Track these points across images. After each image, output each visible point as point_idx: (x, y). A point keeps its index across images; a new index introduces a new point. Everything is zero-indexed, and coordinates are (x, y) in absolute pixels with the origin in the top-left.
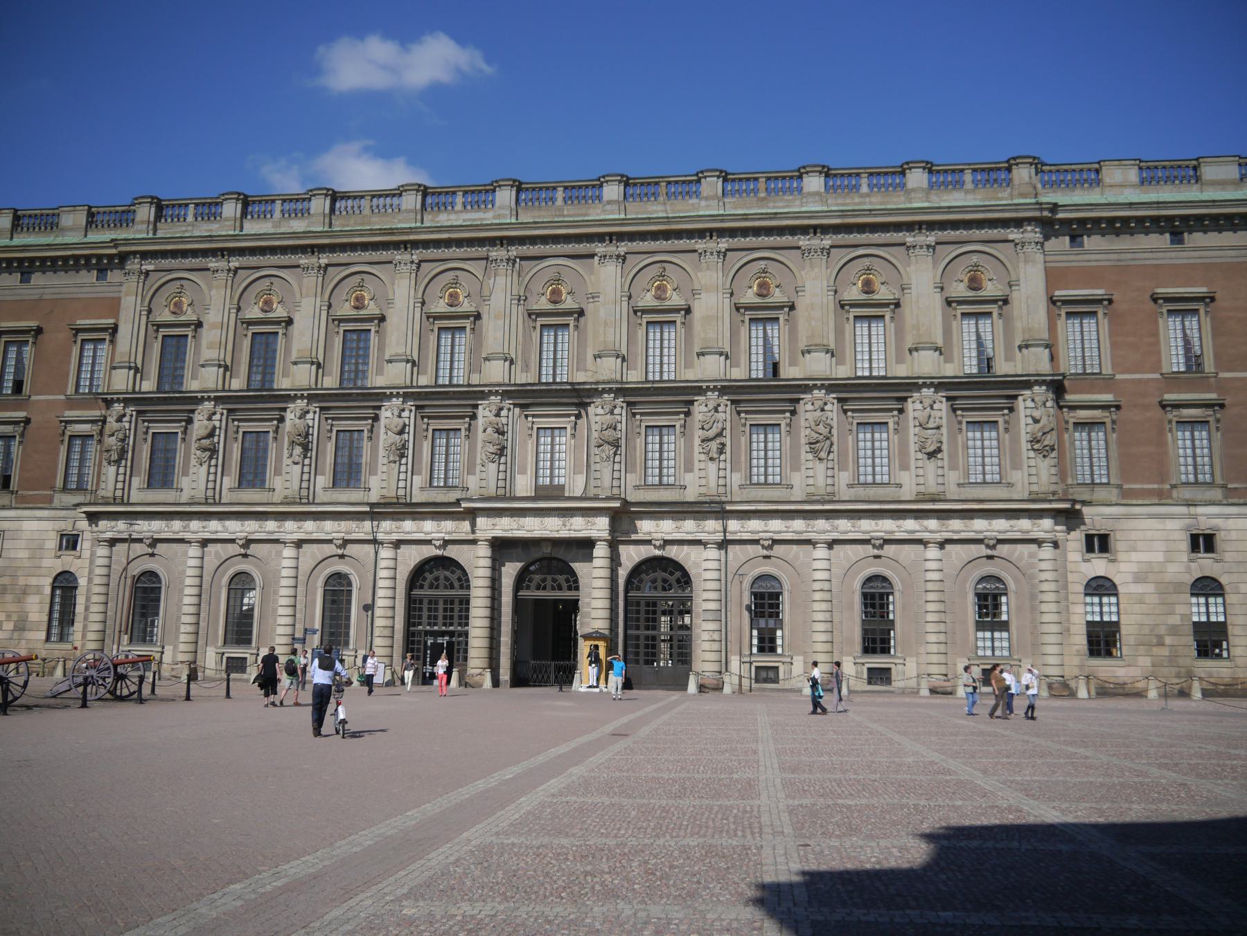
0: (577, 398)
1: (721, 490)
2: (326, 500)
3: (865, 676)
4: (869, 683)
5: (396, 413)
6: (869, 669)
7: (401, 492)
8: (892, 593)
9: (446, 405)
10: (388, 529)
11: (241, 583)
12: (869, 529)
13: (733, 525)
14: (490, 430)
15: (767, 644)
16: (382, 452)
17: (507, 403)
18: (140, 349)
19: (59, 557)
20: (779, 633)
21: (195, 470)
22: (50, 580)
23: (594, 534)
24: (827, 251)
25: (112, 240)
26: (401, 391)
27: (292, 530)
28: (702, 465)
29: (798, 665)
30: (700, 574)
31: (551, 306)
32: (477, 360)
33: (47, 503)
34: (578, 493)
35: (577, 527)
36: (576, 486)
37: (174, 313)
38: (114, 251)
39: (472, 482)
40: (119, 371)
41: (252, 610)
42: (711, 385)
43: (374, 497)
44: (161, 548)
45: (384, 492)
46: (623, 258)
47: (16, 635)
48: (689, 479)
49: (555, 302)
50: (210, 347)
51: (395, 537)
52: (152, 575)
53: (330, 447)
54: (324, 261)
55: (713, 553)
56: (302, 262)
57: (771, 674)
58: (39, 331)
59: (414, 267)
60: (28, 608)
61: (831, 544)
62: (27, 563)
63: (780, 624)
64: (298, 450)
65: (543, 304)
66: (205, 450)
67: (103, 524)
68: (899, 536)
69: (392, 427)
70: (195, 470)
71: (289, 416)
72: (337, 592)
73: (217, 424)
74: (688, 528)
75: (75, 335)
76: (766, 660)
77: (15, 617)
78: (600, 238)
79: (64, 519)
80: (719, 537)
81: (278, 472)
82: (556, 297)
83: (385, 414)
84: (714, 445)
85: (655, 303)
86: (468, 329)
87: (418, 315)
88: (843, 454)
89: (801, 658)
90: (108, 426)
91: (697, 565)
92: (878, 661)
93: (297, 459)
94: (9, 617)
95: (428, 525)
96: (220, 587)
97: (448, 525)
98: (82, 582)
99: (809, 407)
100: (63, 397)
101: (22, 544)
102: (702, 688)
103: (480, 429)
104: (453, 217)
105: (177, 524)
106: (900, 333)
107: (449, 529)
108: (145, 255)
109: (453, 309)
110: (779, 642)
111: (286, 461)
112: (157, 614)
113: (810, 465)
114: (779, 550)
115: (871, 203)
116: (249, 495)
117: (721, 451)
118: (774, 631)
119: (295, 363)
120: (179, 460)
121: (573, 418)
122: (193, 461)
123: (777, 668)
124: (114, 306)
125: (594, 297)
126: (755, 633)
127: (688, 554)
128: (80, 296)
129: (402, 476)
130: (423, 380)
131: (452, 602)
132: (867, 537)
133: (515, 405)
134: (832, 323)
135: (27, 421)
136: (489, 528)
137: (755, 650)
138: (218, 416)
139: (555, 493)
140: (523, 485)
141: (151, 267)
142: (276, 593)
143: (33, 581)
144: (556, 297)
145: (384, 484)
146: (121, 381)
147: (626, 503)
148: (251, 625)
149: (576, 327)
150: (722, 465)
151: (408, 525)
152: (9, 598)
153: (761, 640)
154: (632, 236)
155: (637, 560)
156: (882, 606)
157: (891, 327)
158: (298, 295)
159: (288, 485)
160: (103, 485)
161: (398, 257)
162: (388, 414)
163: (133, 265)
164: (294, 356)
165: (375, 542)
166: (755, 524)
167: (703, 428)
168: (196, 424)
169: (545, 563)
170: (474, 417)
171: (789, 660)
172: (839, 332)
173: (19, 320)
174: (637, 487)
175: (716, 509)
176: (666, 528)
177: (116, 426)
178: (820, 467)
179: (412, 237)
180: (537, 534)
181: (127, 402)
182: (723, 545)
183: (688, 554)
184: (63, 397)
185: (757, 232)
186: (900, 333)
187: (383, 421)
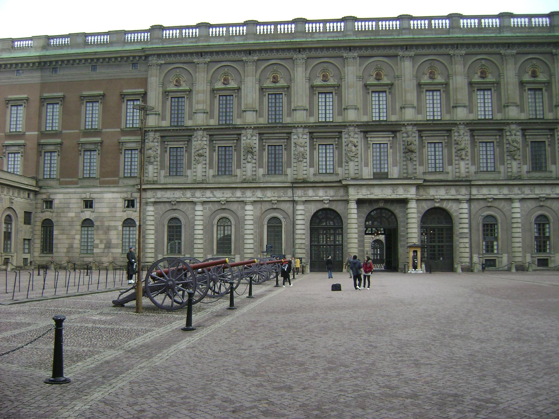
0: (393, 129)
1: (467, 174)
2: (264, 180)
3: (536, 263)
4: (539, 266)
5: (301, 136)
6: (538, 259)
7: (305, 176)
8: (549, 224)
9: (326, 134)
10: (299, 195)
11: (224, 222)
12: (539, 193)
13: (474, 191)
14: (350, 145)
15: (489, 248)
16: (293, 157)
17: (357, 130)
18: (161, 105)
19: (125, 211)
20: (495, 243)
21: (195, 166)
22: (121, 223)
23: (409, 196)
24: (513, 55)
25: (143, 49)
26: (303, 125)
27: (249, 196)
28: (457, 162)
29: (505, 259)
30: (458, 216)
31: (376, 82)
32: (342, 110)
33: (115, 184)
34: (396, 176)
35: (400, 193)
36: (394, 172)
37: (176, 86)
38: (143, 54)
39: (340, 170)
40: (150, 116)
41: (230, 236)
42: (462, 122)
43: (290, 178)
44: (181, 207)
45: (295, 176)
47: (106, 251)
48: (449, 169)
49: (378, 80)
50: (198, 103)
51: (304, 199)
53: (265, 154)
54: (256, 58)
55: (465, 205)
56: (244, 58)
57: (492, 263)
58: (104, 95)
59: (304, 61)
60: (111, 237)
62: (108, 215)
63: (496, 239)
64: (250, 156)
65: (372, 81)
66: (200, 155)
67: (149, 194)
68: (552, 196)
69: (299, 144)
70: (195, 166)
71: (243, 138)
72: (274, 227)
73: (205, 142)
74: (453, 193)
75: (123, 98)
77: (104, 242)
78: (402, 47)
79: (126, 192)
80: (467, 197)
81: (239, 166)
82: (378, 77)
83: (294, 137)
84: (463, 153)
85: (430, 81)
86: (334, 93)
87: (308, 86)
89: (506, 255)
90: (147, 144)
91: (456, 211)
93: (250, 160)
94: (101, 242)
95: (321, 194)
96: (213, 226)
97: (331, 192)
99: (508, 134)
100: (119, 130)
101: (105, 205)
102: (463, 270)
103: (344, 144)
104: (321, 35)
105: (188, 194)
106: (550, 97)
108: (159, 55)
109: (325, 83)
110: (495, 247)
111: (242, 161)
112: (180, 239)
113: (509, 162)
114: (496, 204)
115: (534, 32)
116: (225, 179)
117: (466, 155)
118: (492, 243)
119: (245, 111)
120: (185, 161)
121: (391, 139)
122: (193, 162)
123: (495, 260)
124: (144, 82)
125: (398, 77)
126: (484, 243)
127: (451, 206)
128: (123, 77)
129: (305, 168)
130: (312, 120)
131: (442, 230)
132: (538, 197)
133: (361, 132)
134: (518, 92)
135: (101, 143)
136: (354, 194)
137: (484, 252)
138: (205, 139)
139: (384, 176)
140: (367, 172)
141: (163, 62)
142: (243, 228)
143: (112, 224)
144: (378, 77)
145: (295, 173)
146: (152, 121)
147: (425, 181)
148: (230, 243)
149: (390, 92)
150: (467, 162)
151: (310, 192)
152: (100, 232)
153: (487, 246)
154: (417, 46)
155: (427, 209)
156: (491, 230)
157: (546, 94)
158: (242, 76)
159: (244, 173)
160: (146, 175)
161: (295, 56)
162: (295, 137)
163: (153, 60)
164: (243, 108)
165: (294, 202)
166: (485, 191)
167: (457, 144)
168: (194, 143)
169: (379, 211)
170: (340, 138)
171: (501, 256)
172: (521, 97)
173: (91, 90)
174: (424, 173)
175: (467, 183)
176: (441, 193)
177: (151, 144)
178: (515, 164)
179: (303, 46)
180: (380, 197)
181: (156, 131)
182: (470, 201)
183: (451, 206)
184: (119, 130)
185: (480, 45)
186: (550, 97)
187: (293, 141)
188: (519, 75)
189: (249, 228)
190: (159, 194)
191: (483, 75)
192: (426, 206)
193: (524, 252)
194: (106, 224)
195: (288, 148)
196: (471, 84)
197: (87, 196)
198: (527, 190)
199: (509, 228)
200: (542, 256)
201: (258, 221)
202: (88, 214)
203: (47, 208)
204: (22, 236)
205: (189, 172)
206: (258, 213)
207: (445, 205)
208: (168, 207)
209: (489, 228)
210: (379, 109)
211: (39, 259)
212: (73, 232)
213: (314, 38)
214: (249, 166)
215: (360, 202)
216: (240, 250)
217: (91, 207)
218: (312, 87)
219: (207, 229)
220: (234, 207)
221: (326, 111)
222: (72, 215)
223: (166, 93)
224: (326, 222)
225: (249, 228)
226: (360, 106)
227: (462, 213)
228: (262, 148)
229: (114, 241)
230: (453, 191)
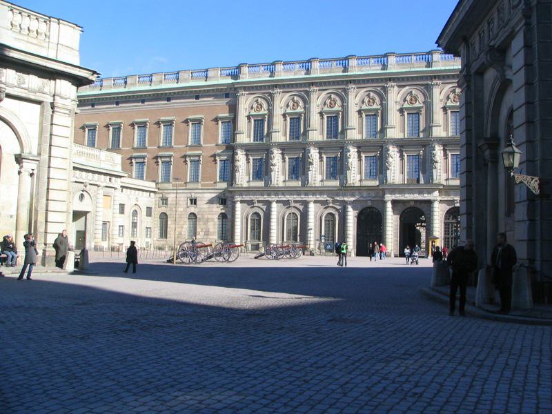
35: (426, 197)
62: (207, 210)
98: (229, 217)
107: (373, 195)
143: (210, 217)
194: (206, 217)
197: (193, 195)
202: (192, 209)
203: (163, 204)
204: (145, 225)
211: (157, 242)
212: (182, 223)
213: (362, 71)
215: (394, 202)
217: (195, 203)
222: (181, 209)
223: (249, 117)
229: (211, 230)
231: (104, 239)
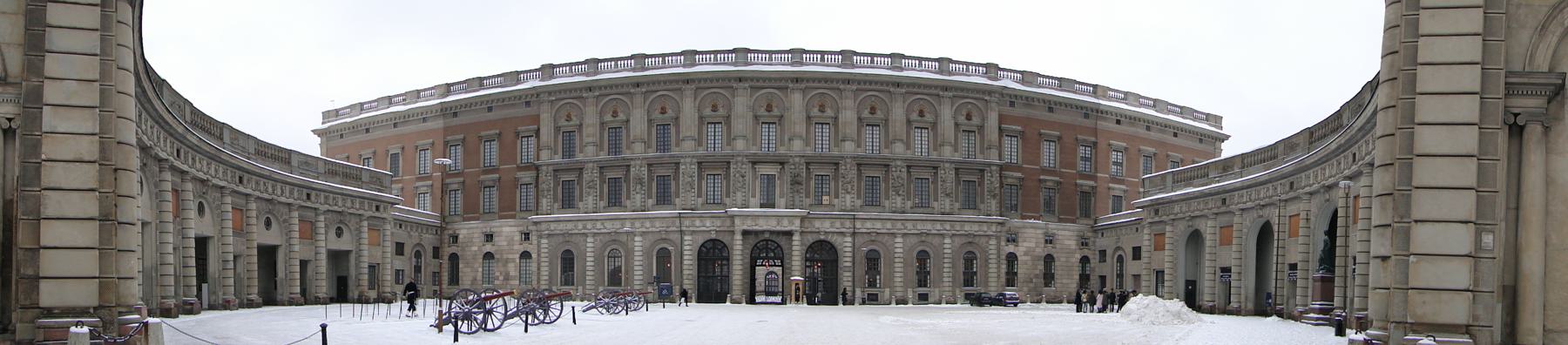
9: (715, 167)
11: (613, 256)
15: (872, 284)
46: (804, 91)
52: (568, 251)
55: (849, 239)
61: (904, 235)
72: (663, 256)
76: (873, 291)
81: (628, 198)
82: (769, 108)
88: (909, 193)
92: (922, 290)
97: (718, 223)
105: (580, 226)
106: (936, 135)
114: (880, 238)
120: (577, 193)
130: (701, 151)
136: (740, 226)
151: (698, 223)
166: (869, 224)
178: (899, 199)
186: (936, 135)
188: (908, 111)
189: (638, 258)
190: (553, 226)
191: (873, 111)
192: (811, 239)
193: (906, 286)
195: (676, 178)
196: (860, 119)
198: (909, 225)
199: (891, 264)
200: (922, 290)
201: (647, 253)
205: (581, 205)
206: (648, 244)
207: (829, 238)
208: (561, 239)
209: (873, 261)
210: (768, 142)
214: (638, 197)
215: (745, 233)
216: (629, 281)
218: (701, 118)
219: (598, 260)
220: (624, 238)
221: (716, 141)
224: (712, 254)
225: (638, 258)
226: (750, 136)
227: (845, 245)
228: (650, 179)
230: (838, 224)
231: (371, 287)
